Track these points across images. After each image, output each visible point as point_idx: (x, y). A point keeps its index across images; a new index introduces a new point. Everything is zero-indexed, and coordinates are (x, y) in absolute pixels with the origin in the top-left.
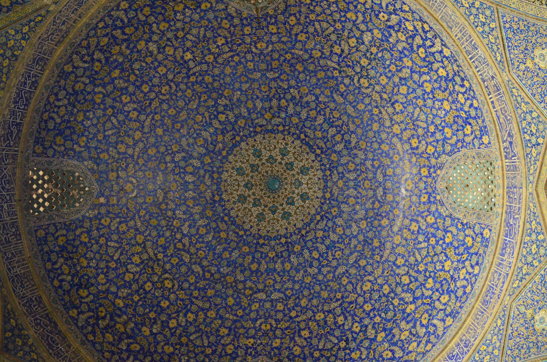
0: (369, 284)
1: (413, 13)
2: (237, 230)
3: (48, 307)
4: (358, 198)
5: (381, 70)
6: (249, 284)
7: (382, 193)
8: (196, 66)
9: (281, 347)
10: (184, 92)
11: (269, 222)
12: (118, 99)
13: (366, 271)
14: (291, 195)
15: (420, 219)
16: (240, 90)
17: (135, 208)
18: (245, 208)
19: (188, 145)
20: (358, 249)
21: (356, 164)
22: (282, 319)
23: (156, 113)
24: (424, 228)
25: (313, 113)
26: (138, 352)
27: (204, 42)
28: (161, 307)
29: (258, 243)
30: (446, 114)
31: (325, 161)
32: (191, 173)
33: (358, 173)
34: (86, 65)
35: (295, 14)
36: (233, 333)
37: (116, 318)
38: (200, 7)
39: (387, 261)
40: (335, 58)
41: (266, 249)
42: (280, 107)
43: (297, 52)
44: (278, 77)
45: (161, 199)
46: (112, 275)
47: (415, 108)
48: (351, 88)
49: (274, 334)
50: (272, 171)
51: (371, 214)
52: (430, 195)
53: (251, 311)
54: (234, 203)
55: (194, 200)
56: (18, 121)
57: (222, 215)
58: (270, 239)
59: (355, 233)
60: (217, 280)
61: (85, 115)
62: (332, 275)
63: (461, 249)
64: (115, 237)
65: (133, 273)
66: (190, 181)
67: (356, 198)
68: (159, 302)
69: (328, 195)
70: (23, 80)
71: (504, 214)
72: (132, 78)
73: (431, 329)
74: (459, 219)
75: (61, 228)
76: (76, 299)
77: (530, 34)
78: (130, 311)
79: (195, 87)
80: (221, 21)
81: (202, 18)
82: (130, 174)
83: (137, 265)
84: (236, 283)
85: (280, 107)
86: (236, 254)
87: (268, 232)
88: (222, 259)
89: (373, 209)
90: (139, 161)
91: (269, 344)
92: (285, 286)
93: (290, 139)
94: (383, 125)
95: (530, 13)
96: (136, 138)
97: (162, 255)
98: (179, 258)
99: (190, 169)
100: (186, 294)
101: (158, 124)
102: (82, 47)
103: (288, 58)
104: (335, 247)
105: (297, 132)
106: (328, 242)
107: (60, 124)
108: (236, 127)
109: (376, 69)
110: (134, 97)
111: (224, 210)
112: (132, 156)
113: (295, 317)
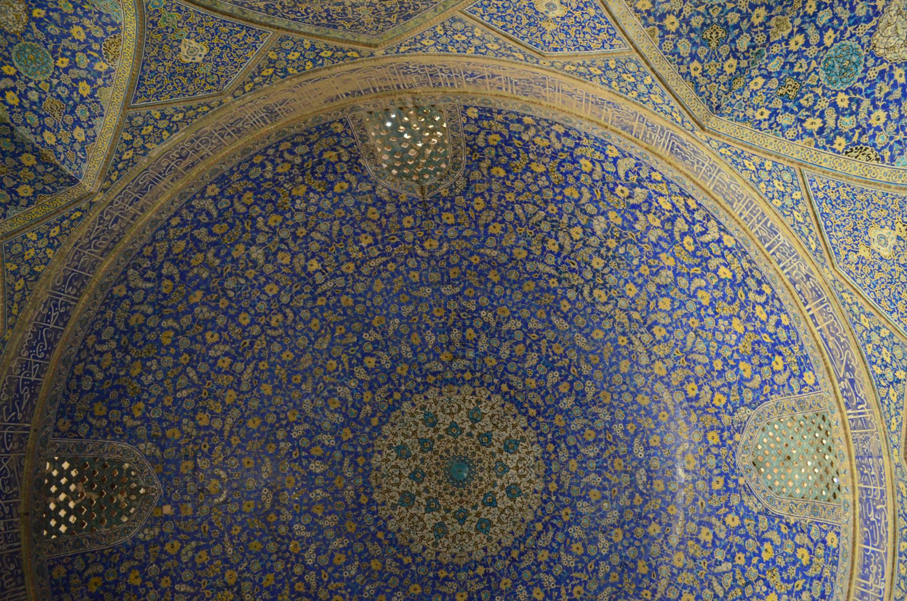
1: (668, 183)
2: (400, 556)
4: (605, 489)
5: (626, 274)
8: (327, 280)
10: (307, 322)
11: (454, 538)
14: (490, 489)
15: (714, 520)
16: (399, 316)
17: (223, 522)
18: (412, 516)
19: (315, 410)
20: (611, 580)
21: (596, 431)
23: (261, 359)
24: (722, 535)
25: (520, 349)
27: (339, 242)
29: (437, 577)
30: (738, 340)
31: (545, 428)
32: (319, 458)
33: (602, 445)
34: (149, 285)
35: (482, 194)
38: (332, 189)
42: (464, 342)
43: (488, 251)
45: (268, 506)
47: (686, 333)
48: (579, 305)
50: (456, 449)
54: (394, 507)
55: (325, 505)
56: (33, 378)
57: (372, 529)
58: (457, 568)
59: (604, 552)
61: (144, 365)
63: (792, 571)
66: (318, 471)
67: (602, 488)
69: (553, 487)
70: (46, 311)
71: (858, 505)
72: (223, 303)
74: (781, 517)
75: (95, 561)
77: (858, 205)
79: (325, 314)
80: (366, 208)
81: (335, 206)
82: (216, 463)
85: (464, 342)
87: (453, 556)
89: (632, 507)
93: (483, 393)
94: (638, 364)
95: (854, 173)
96: (228, 401)
99: (317, 451)
101: (265, 376)
102: (144, 257)
103: (475, 263)
105: (496, 381)
106: (558, 570)
107: (102, 382)
108: (394, 377)
109: (617, 273)
110: (225, 335)
111: (377, 520)
112: (221, 432)
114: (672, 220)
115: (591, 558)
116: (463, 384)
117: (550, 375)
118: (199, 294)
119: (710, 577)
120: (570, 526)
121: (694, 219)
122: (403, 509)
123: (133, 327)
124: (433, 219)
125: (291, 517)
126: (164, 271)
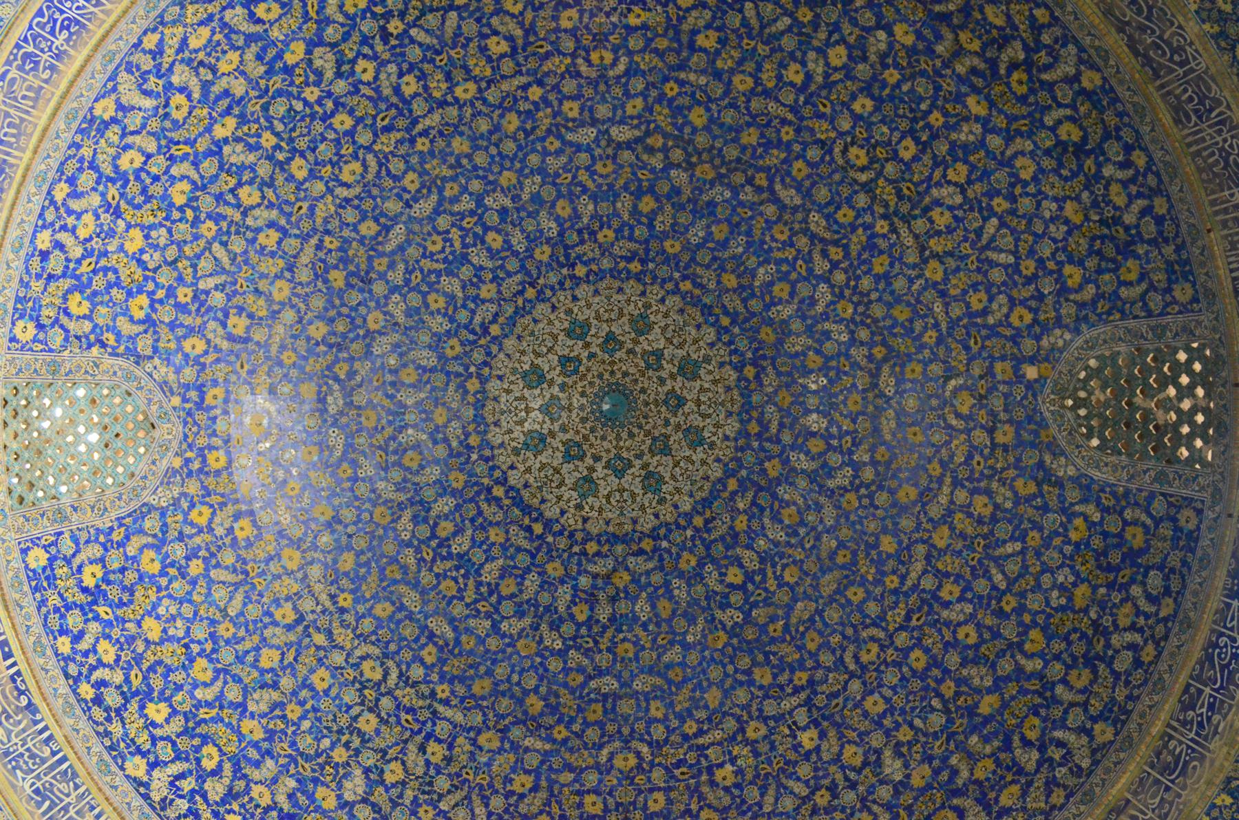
0: (346, 177)
2: (697, 292)
4: (393, 384)
5: (324, 704)
6: (657, 161)
7: (330, 399)
8: (791, 713)
9: (556, 9)
10: (826, 645)
11: (621, 315)
12: (987, 636)
14: (569, 381)
16: (686, 647)
18: (681, 346)
19: (819, 508)
20: (385, 261)
23: (895, 592)
24: (212, 325)
28: (873, 98)
29: (643, 262)
30: (155, 607)
34: (1058, 734)
36: (685, 39)
37: (982, 66)
39: (305, 238)
40: (442, 729)
41: (623, 248)
42: (592, 600)
43: (539, 745)
44: (591, 678)
45: (886, 369)
46: (1001, 177)
47: (242, 614)
48: (407, 655)
49: (578, 41)
50: (618, 438)
51: (357, 347)
52: (200, 405)
54: (707, 360)
57: (737, 330)
58: (614, 273)
59: (396, 297)
61: (1070, 599)
62: (447, 193)
64: (997, 275)
65: (949, 182)
68: (877, 109)
69: (473, 385)
70: (1216, 718)
72: (948, 689)
73: (153, 83)
74: (114, 354)
76: (1088, 116)
78: (948, 85)
83: (938, 203)
86: (696, 234)
88: (728, 220)
89: (352, 359)
90: (938, 471)
92: (564, 159)
93: (571, 521)
94: (326, 565)
96: (945, 530)
100: (812, 131)
101: (891, 564)
102: (1065, 787)
103: (561, 728)
104: (445, 260)
105: (550, 539)
106: (466, 272)
107: (1133, 581)
108: (701, 550)
110: (948, 636)
111: (731, 343)
112: (956, 483)
114: (231, 795)
115: (416, 289)
117: (465, 548)
118: (985, 709)
121: (192, 801)
123: (1085, 665)
124: (618, 805)
125: (853, 351)
126: (1035, 755)
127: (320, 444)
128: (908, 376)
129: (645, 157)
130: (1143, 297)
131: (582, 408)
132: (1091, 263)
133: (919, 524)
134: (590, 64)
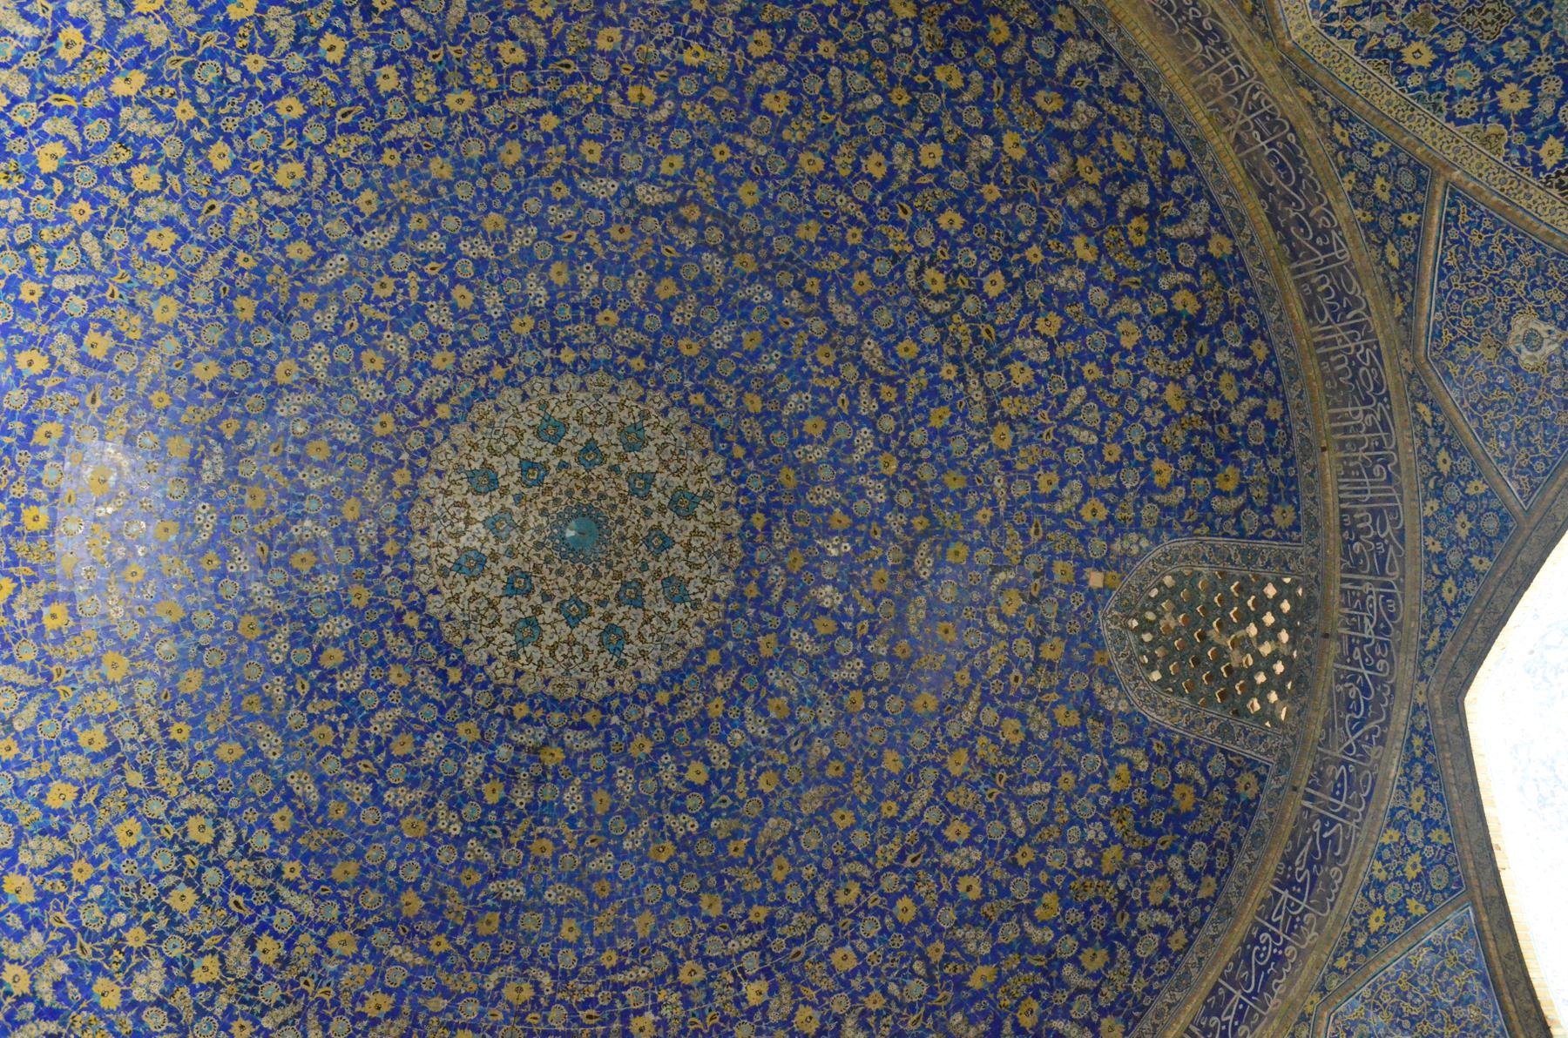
0: (281, 178)
2: (710, 409)
3: (1290, 282)
4: (296, 458)
6: (688, 238)
7: (206, 463)
8: (738, 956)
9: (594, 23)
10: (795, 877)
13: (289, 221)
14: (529, 492)
16: (621, 855)
17: (1003, 534)
18: (678, 473)
19: (815, 702)
20: (314, 296)
21: (287, 565)
22: (588, 108)
23: (891, 822)
24: (62, 338)
25: (402, 746)
26: (1040, 85)
28: (964, 215)
29: (649, 359)
37: (1099, 203)
39: (212, 247)
40: (283, 920)
41: (627, 337)
42: (509, 777)
43: (408, 957)
44: (491, 878)
45: (924, 546)
47: (32, 730)
48: (252, 816)
49: (615, 69)
50: (579, 575)
53: (686, 153)
54: (708, 496)
55: (826, 526)
57: (751, 466)
58: (611, 367)
59: (320, 347)
60: (784, 267)
61: (1098, 861)
62: (413, 226)
64: (1074, 456)
65: (1037, 333)
66: (829, 588)
68: (967, 228)
69: (402, 477)
72: (936, 951)
75: (1225, 518)
76: (1210, 287)
78: (1056, 218)
79: (758, 886)
83: (1020, 356)
84: (728, 248)
85: (509, 777)
86: (722, 337)
91: (632, 40)
92: (571, 212)
93: (500, 672)
94: (162, 681)
96: (963, 755)
97: (943, 373)
98: (895, 355)
100: (885, 239)
103: (442, 938)
104: (394, 311)
105: (468, 691)
106: (418, 331)
107: (1173, 850)
108: (660, 734)
109: (147, 874)
111: (741, 480)
112: (986, 699)
113: (543, 110)
116: (534, 696)
118: (975, 982)
119: (105, 270)
120: (381, 403)
122: (693, 489)
125: (888, 517)
127: (182, 520)
128: (950, 558)
129: (674, 230)
130: (1237, 512)
131: (539, 529)
132: (1185, 462)
133: (934, 743)
134: (626, 102)
